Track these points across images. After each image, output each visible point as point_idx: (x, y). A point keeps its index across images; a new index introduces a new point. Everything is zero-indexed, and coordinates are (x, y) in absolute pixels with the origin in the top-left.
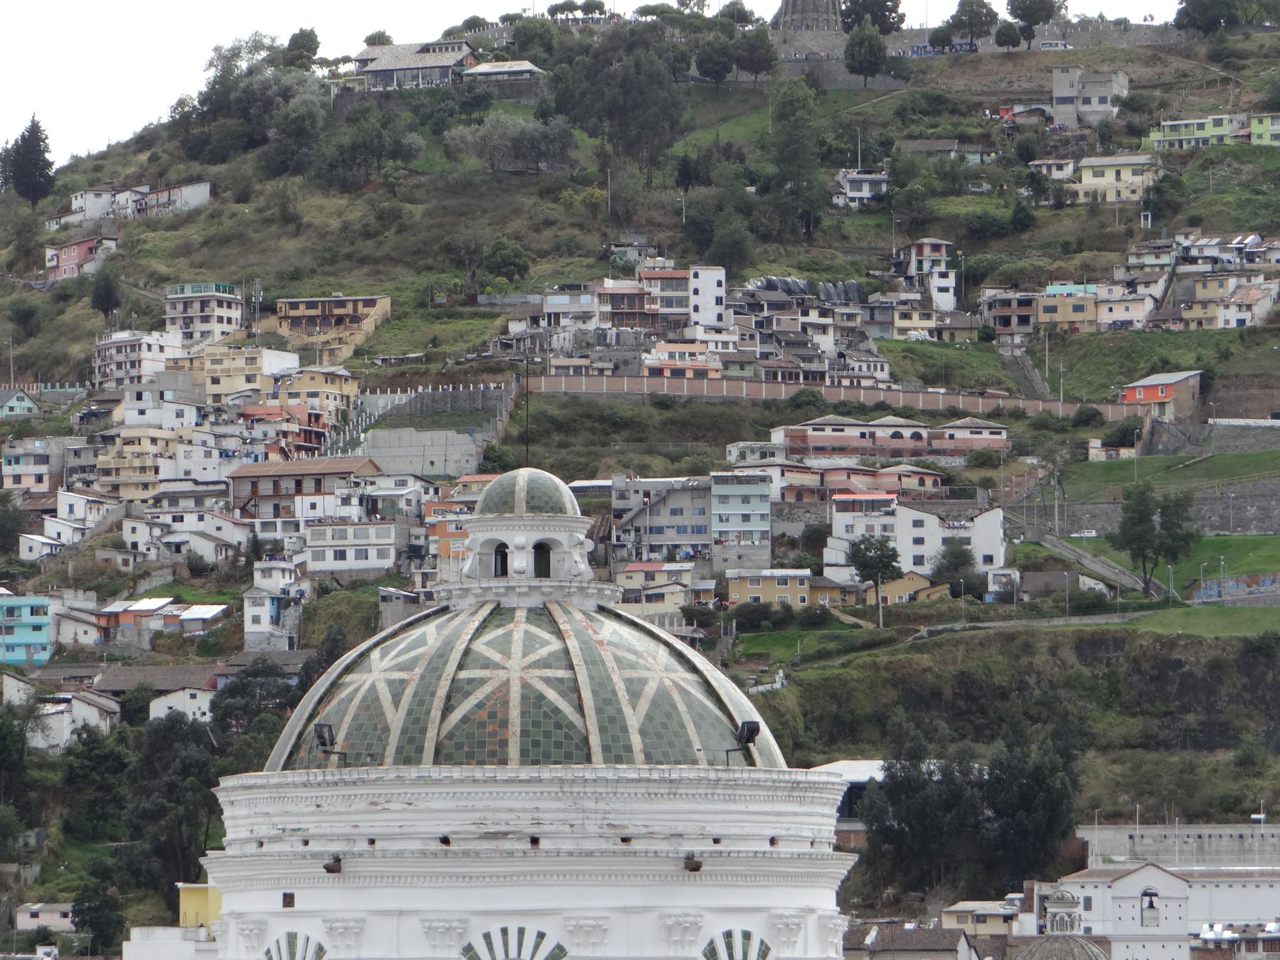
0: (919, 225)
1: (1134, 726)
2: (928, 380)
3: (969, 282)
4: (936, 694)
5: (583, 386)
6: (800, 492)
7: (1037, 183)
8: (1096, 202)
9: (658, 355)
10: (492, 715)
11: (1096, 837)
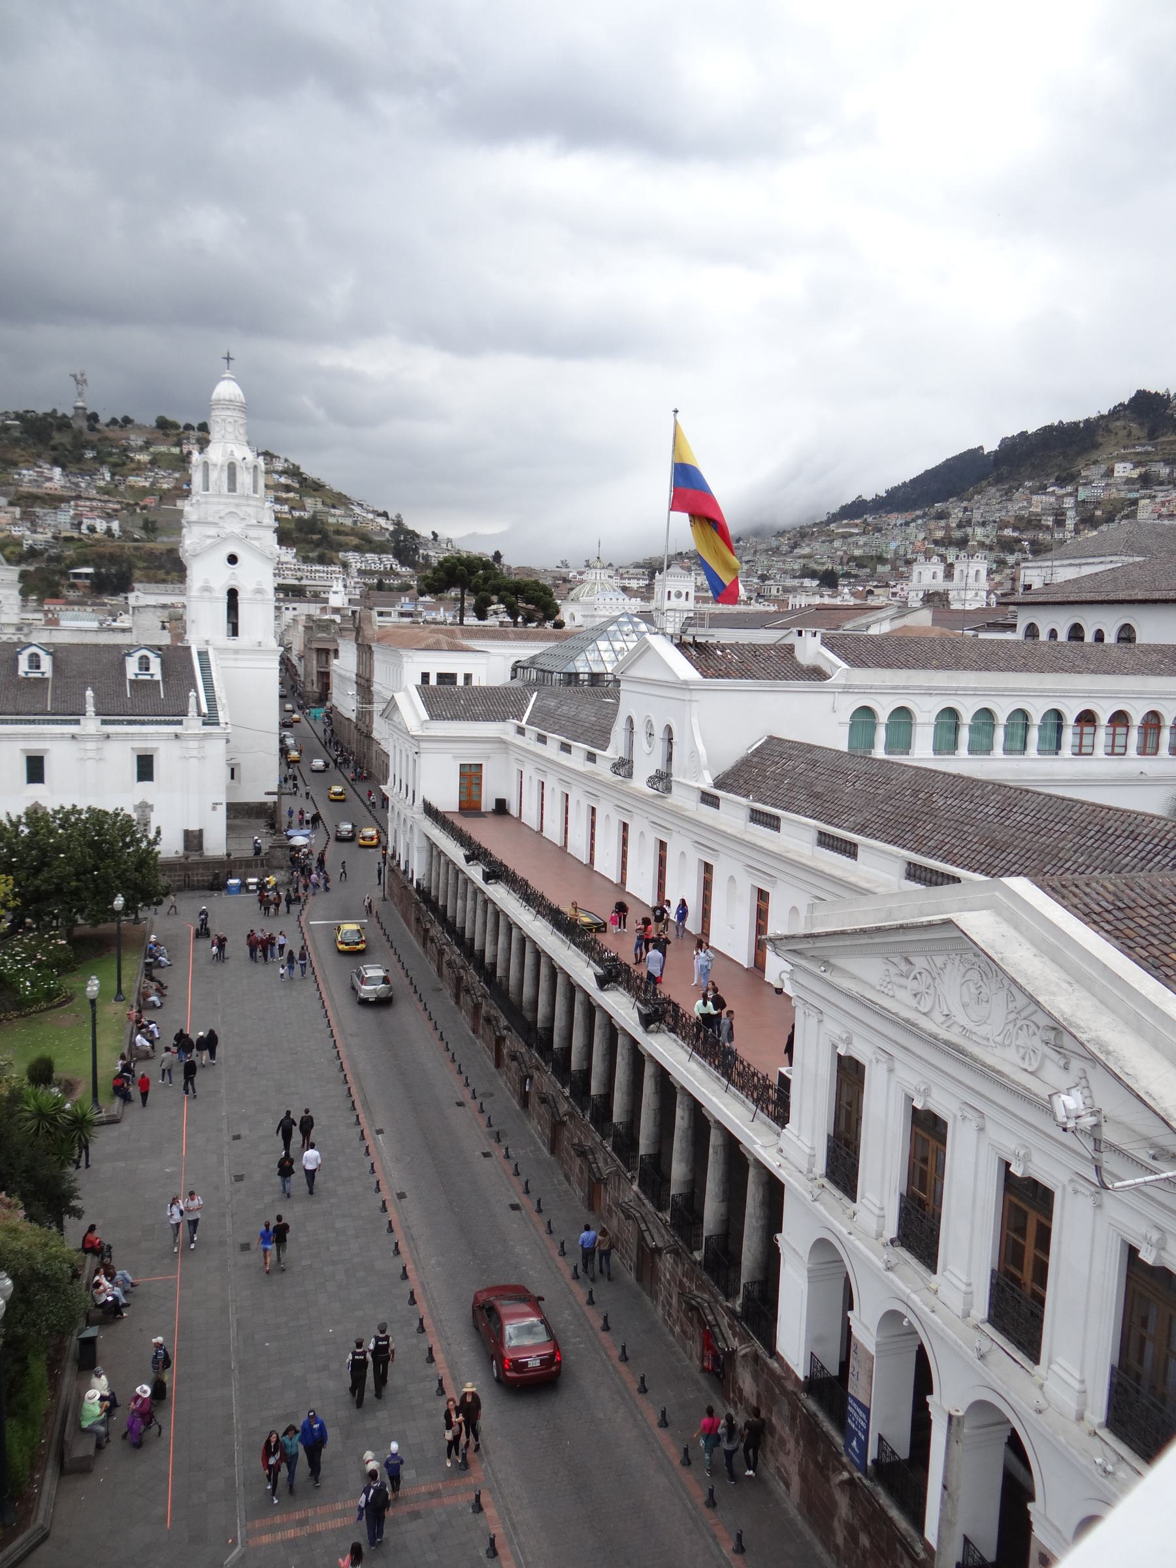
0: (102, 463)
1: (145, 565)
2: (105, 494)
3: (113, 475)
4: (105, 556)
5: (31, 490)
6: (76, 514)
7: (128, 457)
8: (139, 461)
9: (48, 484)
11: (136, 585)
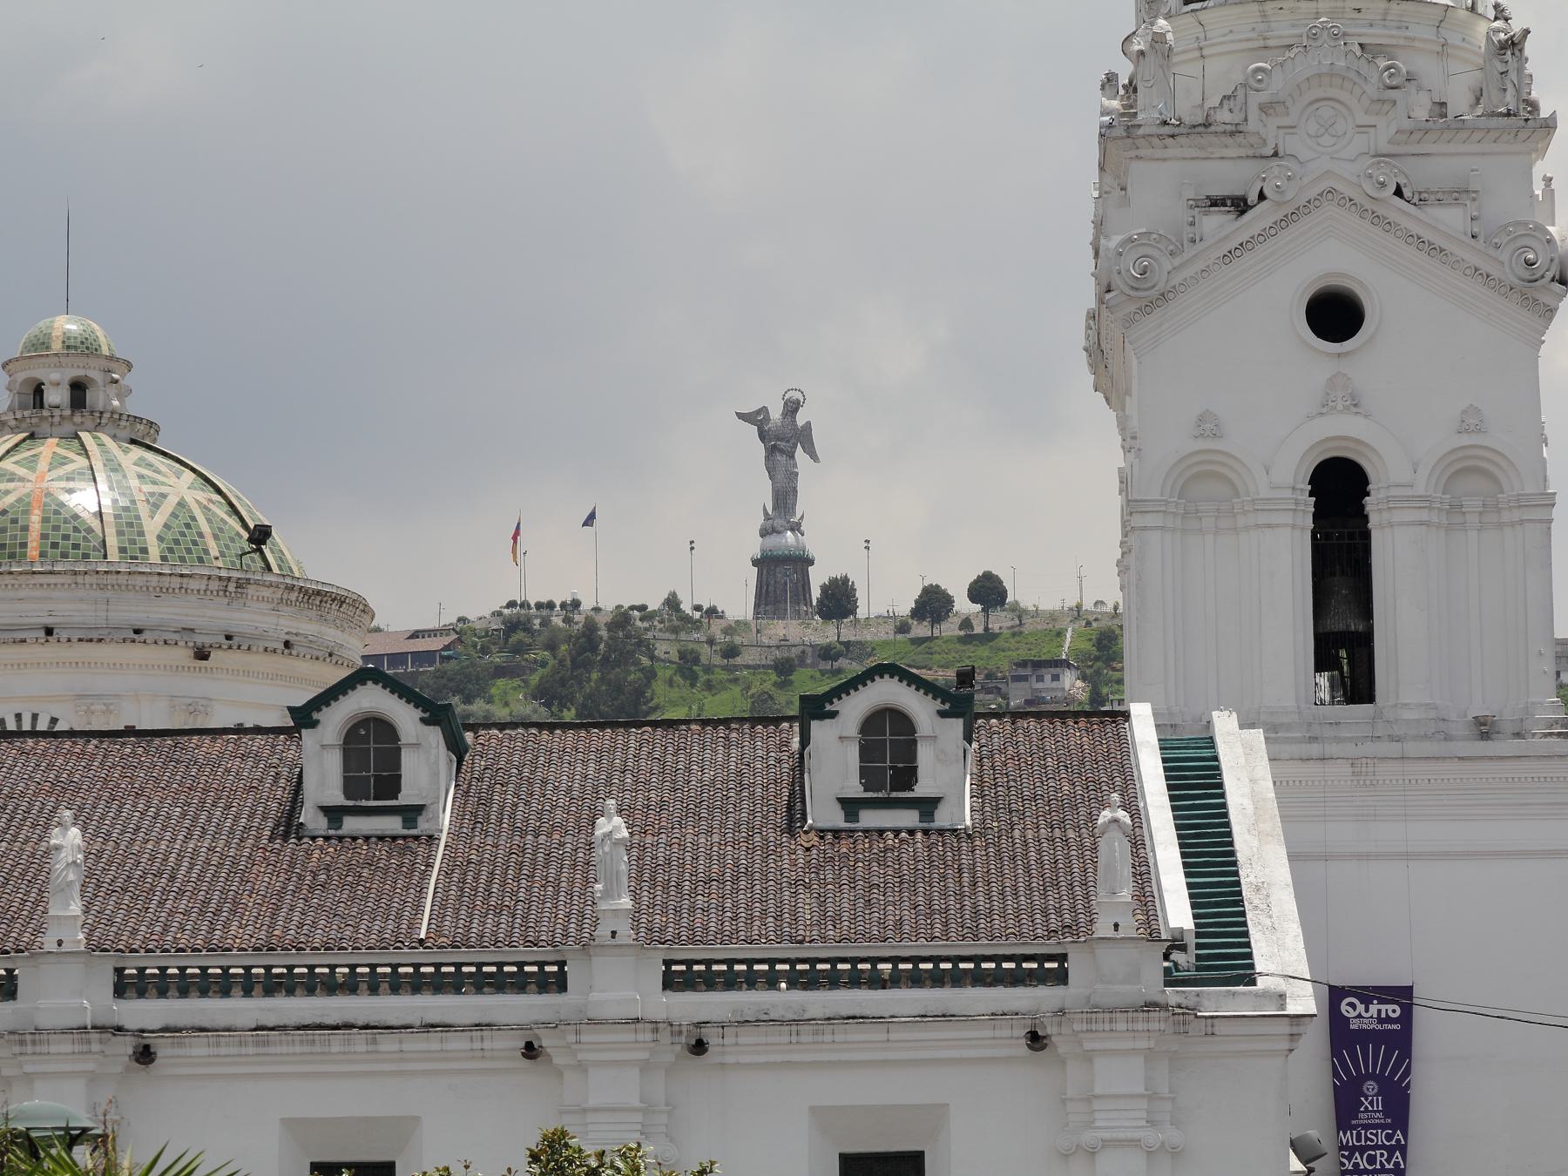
10: (14, 521)
